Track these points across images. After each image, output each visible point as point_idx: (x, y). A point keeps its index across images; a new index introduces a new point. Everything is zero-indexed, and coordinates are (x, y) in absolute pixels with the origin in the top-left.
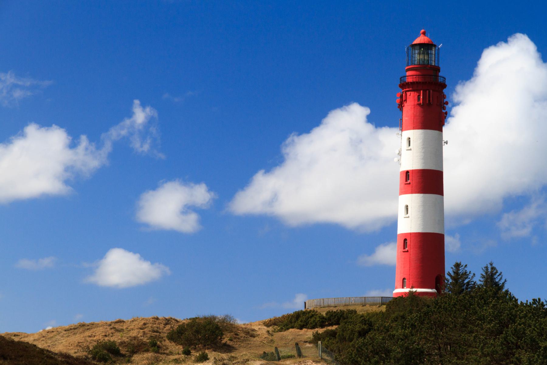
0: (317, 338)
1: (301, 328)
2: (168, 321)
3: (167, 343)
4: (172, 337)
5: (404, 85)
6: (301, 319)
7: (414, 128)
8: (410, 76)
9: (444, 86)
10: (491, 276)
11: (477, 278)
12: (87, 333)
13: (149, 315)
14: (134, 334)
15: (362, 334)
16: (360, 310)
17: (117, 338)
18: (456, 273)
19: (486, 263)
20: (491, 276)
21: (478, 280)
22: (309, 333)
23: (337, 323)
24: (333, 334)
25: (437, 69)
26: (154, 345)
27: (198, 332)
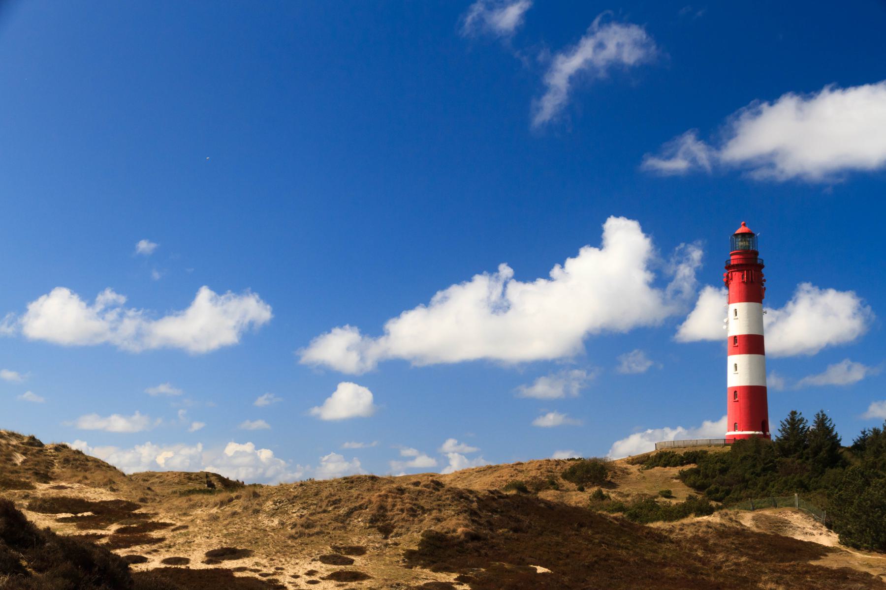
0: (683, 476)
1: (665, 466)
2: (558, 462)
3: (561, 481)
4: (565, 476)
5: (729, 267)
6: (664, 458)
7: (740, 301)
8: (735, 260)
9: (762, 266)
10: (822, 421)
11: (811, 425)
12: (497, 474)
13: (542, 458)
14: (533, 473)
15: (723, 471)
16: (711, 451)
17: (521, 478)
18: (793, 419)
19: (818, 411)
20: (822, 421)
21: (811, 425)
22: (675, 471)
23: (694, 462)
24: (696, 472)
25: (756, 253)
26: (553, 483)
27: (588, 472)
